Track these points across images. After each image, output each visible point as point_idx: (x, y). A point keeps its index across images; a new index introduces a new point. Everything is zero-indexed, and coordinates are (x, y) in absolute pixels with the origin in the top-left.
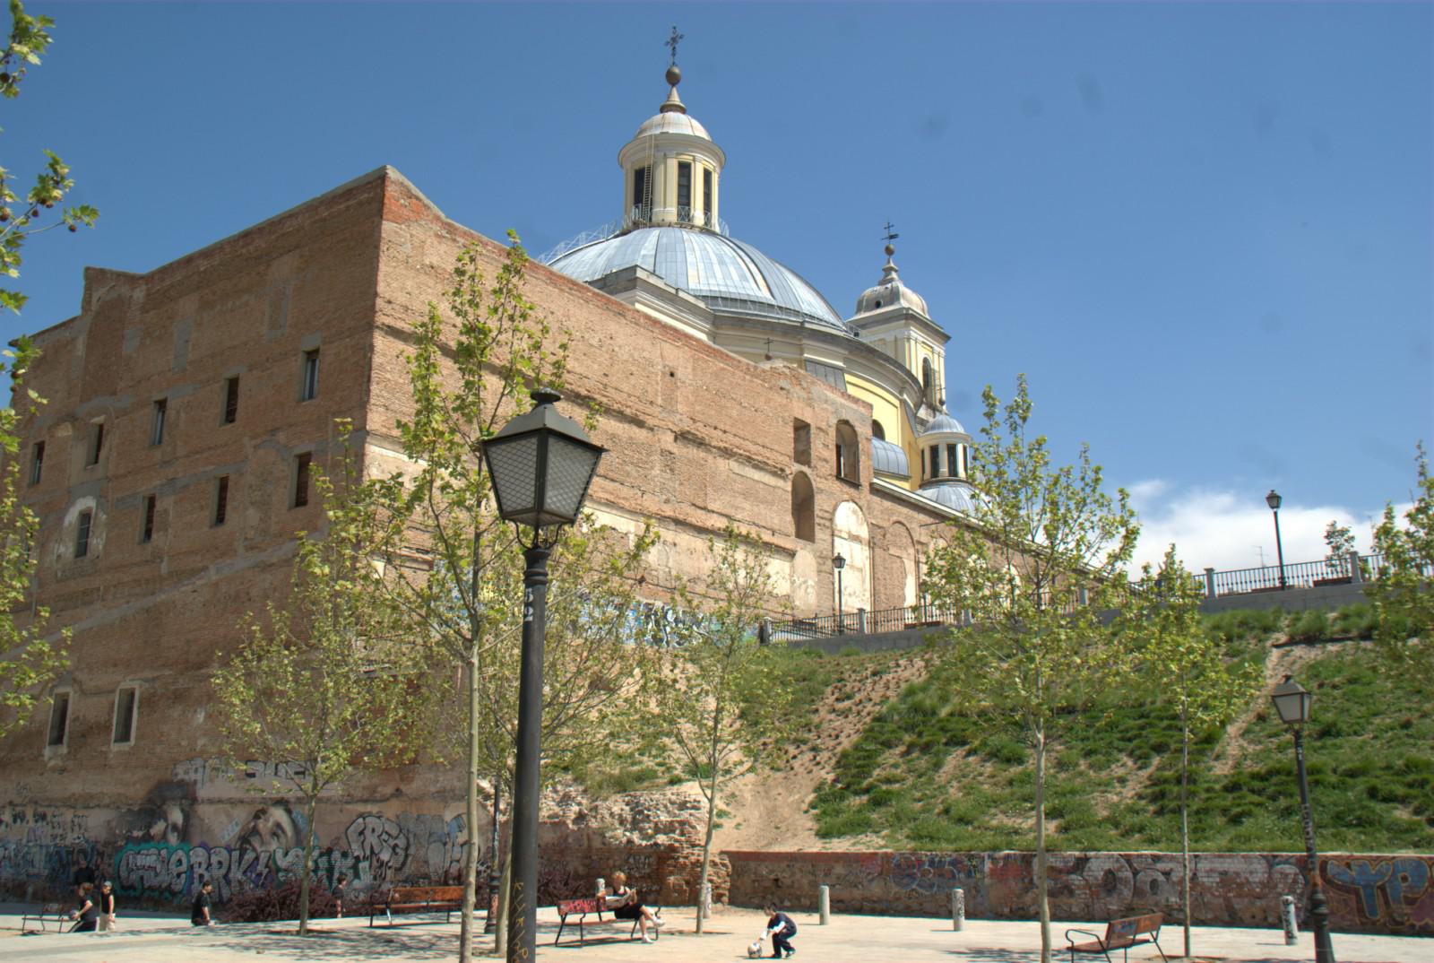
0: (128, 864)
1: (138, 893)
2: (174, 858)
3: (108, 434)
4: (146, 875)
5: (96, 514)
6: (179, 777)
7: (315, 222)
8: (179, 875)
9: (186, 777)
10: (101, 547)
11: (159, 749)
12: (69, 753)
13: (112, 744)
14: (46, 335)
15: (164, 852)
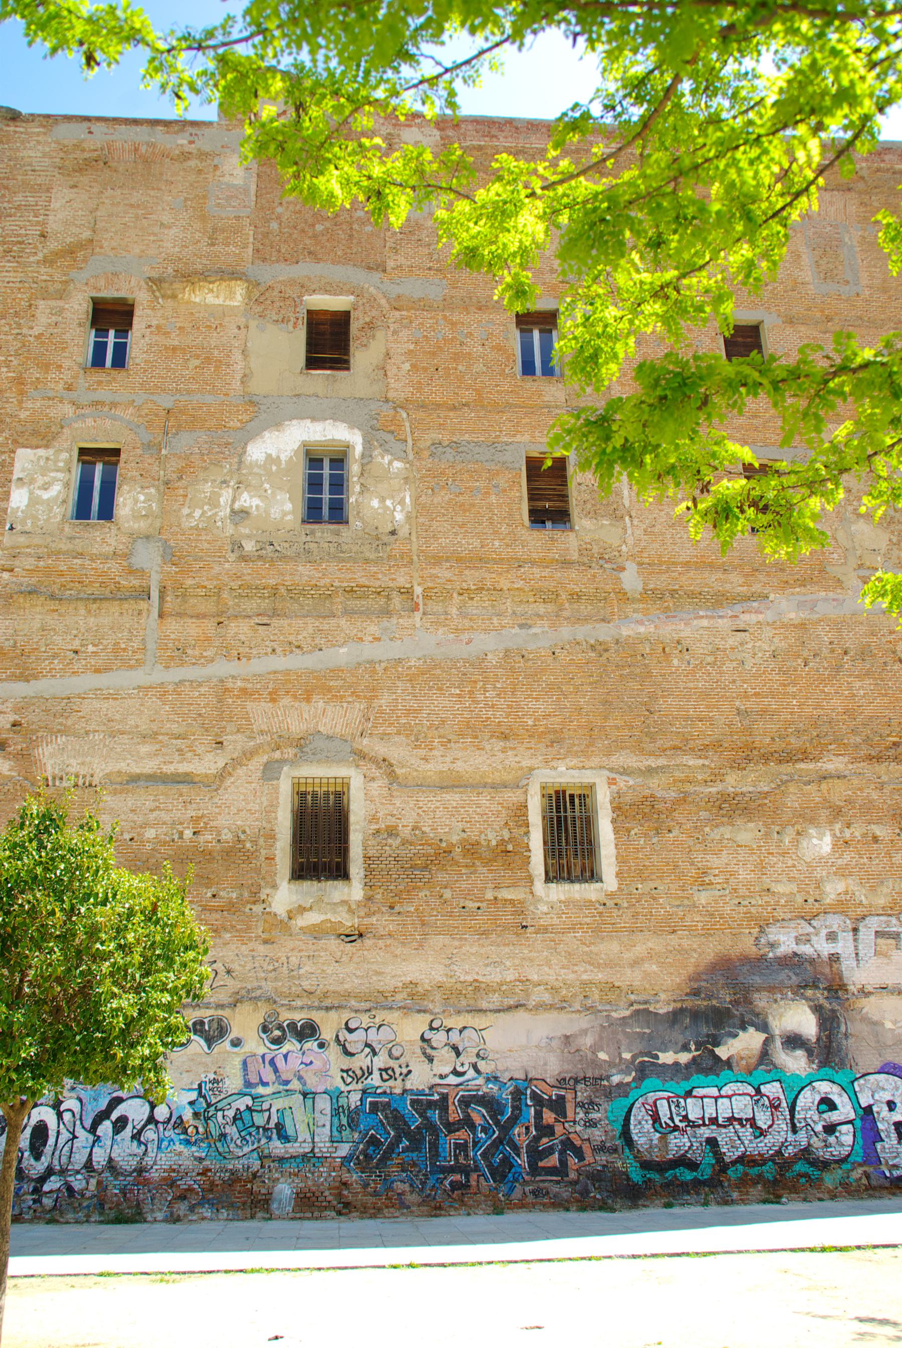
0: (656, 1118)
1: (706, 1172)
2: (808, 1099)
3: (370, 326)
4: (724, 1137)
5: (367, 455)
6: (782, 950)
7: (878, 170)
8: (830, 1129)
9: (805, 950)
10: (399, 516)
11: (703, 898)
12: (369, 899)
13: (539, 886)
14: (97, 128)
15: (772, 1090)
